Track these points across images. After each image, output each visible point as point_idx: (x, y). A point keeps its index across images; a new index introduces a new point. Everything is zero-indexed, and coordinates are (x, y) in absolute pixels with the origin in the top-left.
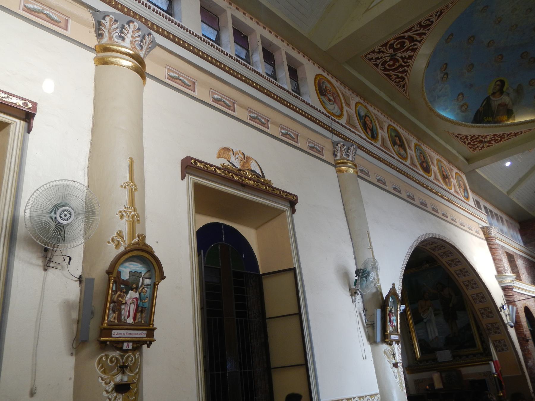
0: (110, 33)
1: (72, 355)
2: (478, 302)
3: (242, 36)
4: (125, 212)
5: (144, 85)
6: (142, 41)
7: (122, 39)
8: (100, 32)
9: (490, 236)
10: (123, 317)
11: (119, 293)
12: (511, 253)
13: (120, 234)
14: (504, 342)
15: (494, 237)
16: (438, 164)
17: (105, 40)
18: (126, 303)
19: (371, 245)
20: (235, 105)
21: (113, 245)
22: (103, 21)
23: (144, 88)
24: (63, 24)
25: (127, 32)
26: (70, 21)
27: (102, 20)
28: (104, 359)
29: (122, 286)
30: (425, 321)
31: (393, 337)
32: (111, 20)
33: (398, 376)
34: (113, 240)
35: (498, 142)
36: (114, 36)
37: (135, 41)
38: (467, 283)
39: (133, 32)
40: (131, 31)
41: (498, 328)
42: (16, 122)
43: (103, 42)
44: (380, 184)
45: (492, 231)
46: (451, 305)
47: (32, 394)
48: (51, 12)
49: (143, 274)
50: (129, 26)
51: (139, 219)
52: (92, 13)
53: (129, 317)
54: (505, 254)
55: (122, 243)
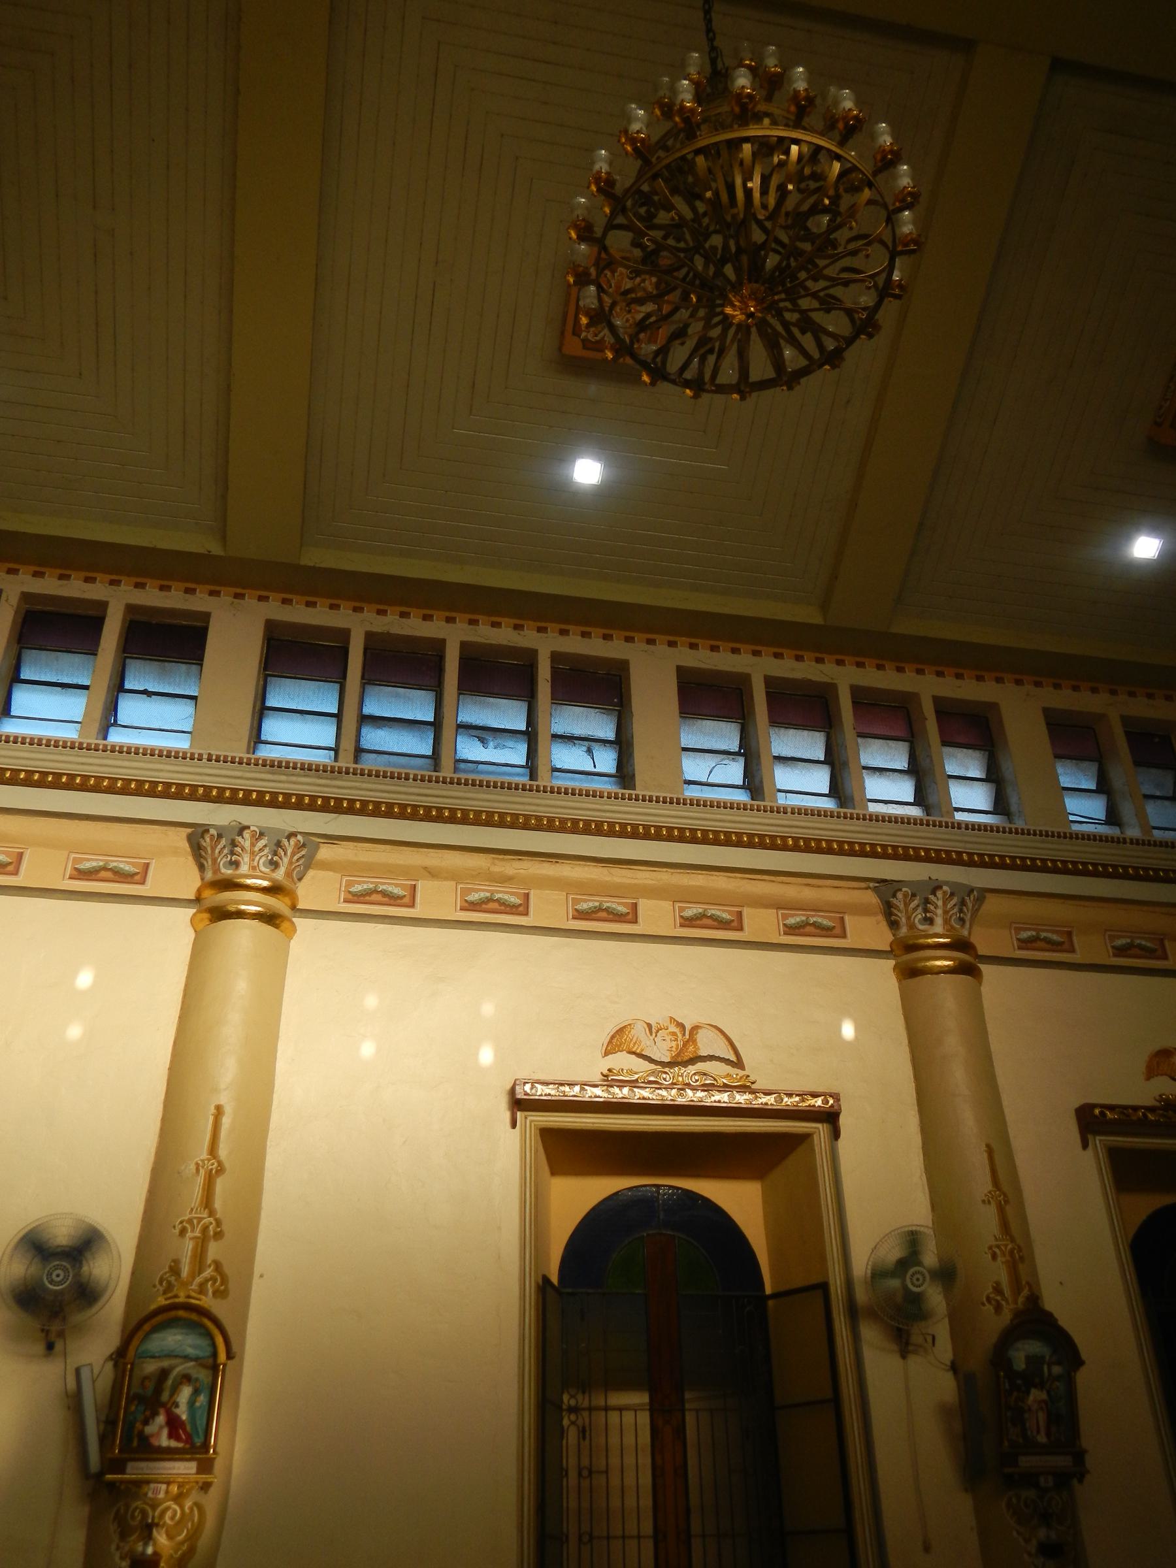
0: (908, 918)
1: (966, 1490)
3: (1157, 740)
4: (998, 1247)
5: (980, 984)
6: (961, 911)
7: (928, 922)
8: (893, 918)
10: (1029, 1433)
11: (1015, 1394)
13: (998, 1289)
17: (904, 931)
18: (1030, 1410)
20: (1167, 943)
21: (989, 1308)
22: (894, 901)
23: (982, 988)
24: (837, 931)
25: (935, 908)
26: (847, 918)
27: (892, 899)
28: (1014, 1500)
29: (1019, 1382)
32: (905, 896)
34: (988, 1299)
36: (916, 921)
37: (951, 917)
39: (945, 904)
40: (940, 903)
42: (818, 1128)
43: (901, 935)
47: (927, 1549)
48: (819, 916)
49: (1047, 1358)
50: (935, 896)
51: (1021, 1254)
52: (875, 889)
53: (1038, 1432)
55: (1003, 1303)
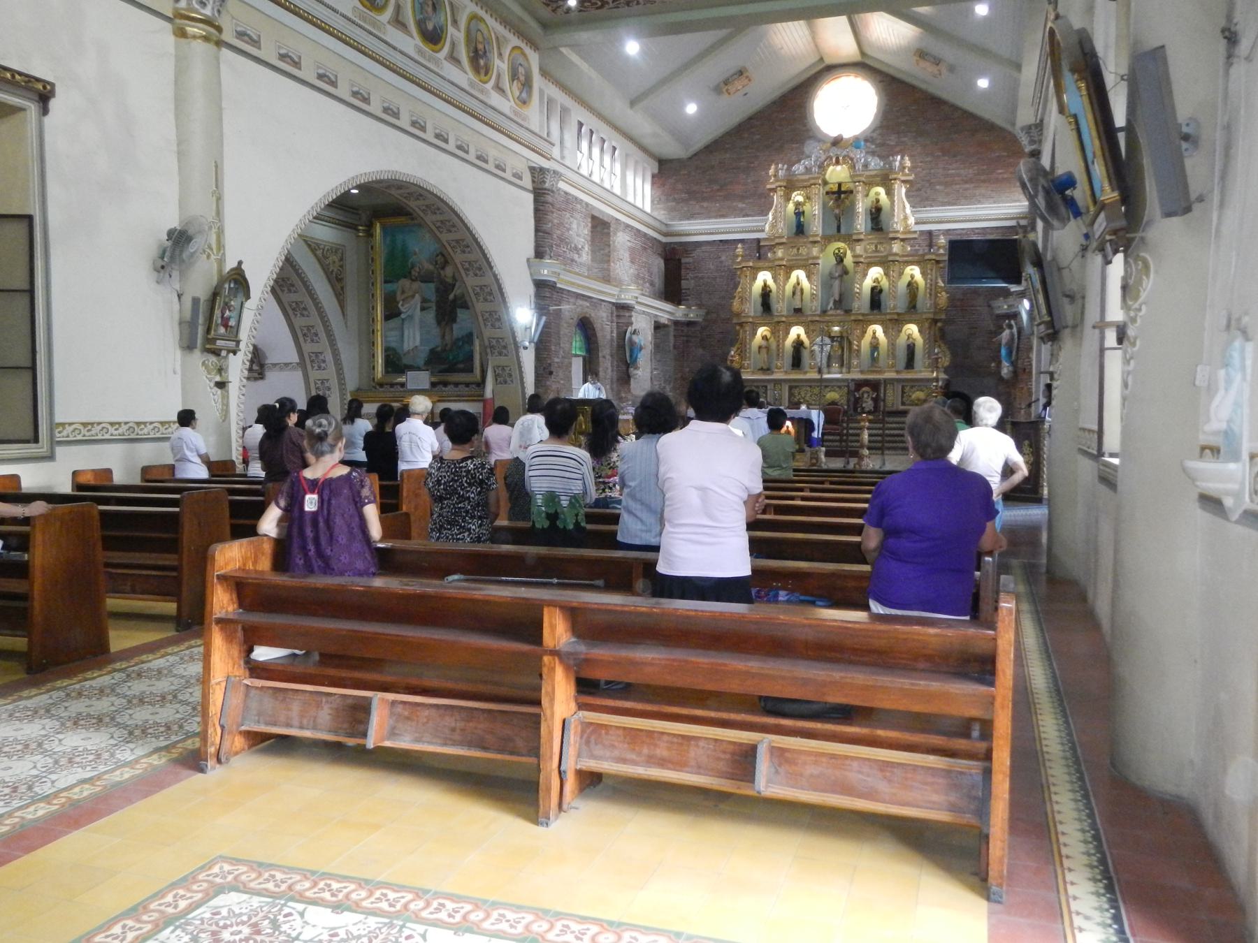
2: (481, 298)
9: (540, 186)
12: (606, 219)
14: (510, 370)
15: (549, 190)
16: (469, 24)
19: (217, 187)
30: (403, 316)
31: (219, 343)
33: (220, 400)
35: (597, 8)
38: (467, 265)
41: (505, 347)
44: (287, 66)
45: (549, 177)
46: (451, 297)
54: (590, 220)
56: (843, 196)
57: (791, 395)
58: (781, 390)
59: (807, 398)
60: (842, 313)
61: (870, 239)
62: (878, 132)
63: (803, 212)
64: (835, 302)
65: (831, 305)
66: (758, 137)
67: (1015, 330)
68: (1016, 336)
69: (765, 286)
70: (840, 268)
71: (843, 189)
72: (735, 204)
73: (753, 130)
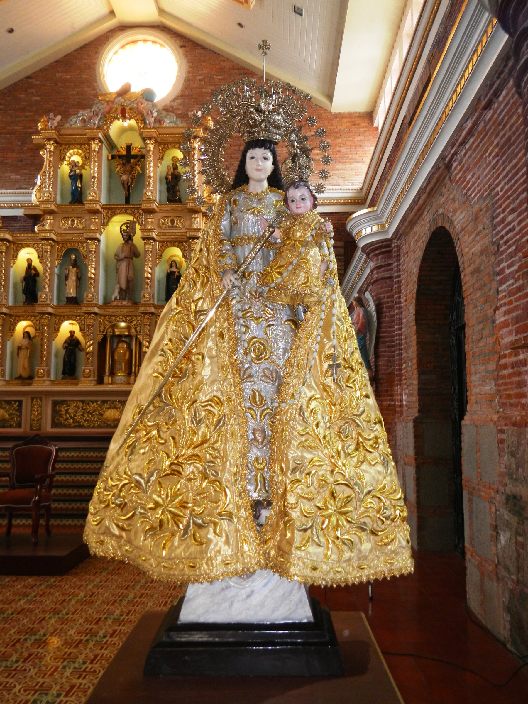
56: (132, 161)
57: (55, 413)
58: (41, 406)
59: (78, 418)
60: (129, 304)
61: (166, 211)
62: (179, 101)
63: (81, 176)
64: (121, 290)
65: (116, 294)
66: (38, 98)
67: (372, 308)
68: (375, 319)
69: (30, 267)
70: (127, 248)
71: (133, 153)
72: (7, 175)
73: (29, 91)
